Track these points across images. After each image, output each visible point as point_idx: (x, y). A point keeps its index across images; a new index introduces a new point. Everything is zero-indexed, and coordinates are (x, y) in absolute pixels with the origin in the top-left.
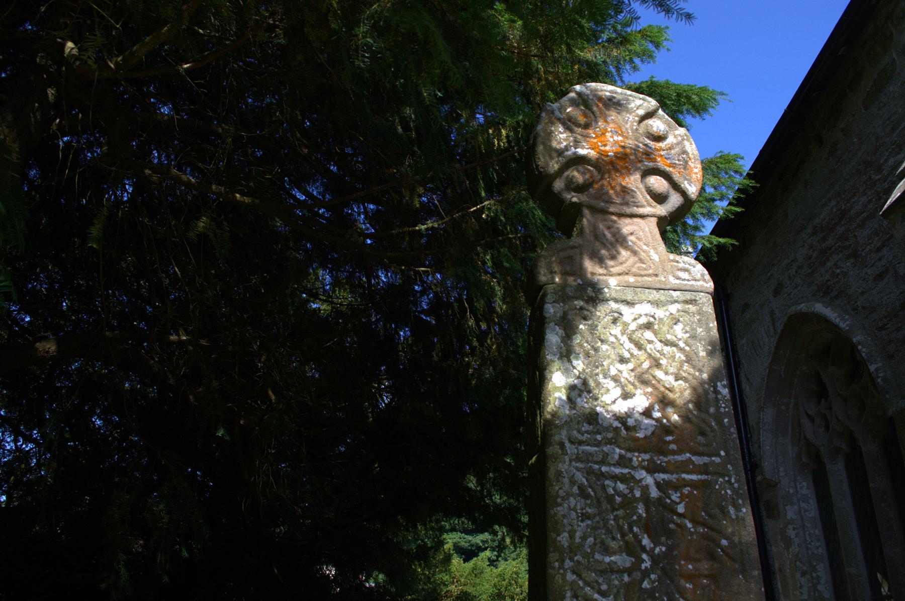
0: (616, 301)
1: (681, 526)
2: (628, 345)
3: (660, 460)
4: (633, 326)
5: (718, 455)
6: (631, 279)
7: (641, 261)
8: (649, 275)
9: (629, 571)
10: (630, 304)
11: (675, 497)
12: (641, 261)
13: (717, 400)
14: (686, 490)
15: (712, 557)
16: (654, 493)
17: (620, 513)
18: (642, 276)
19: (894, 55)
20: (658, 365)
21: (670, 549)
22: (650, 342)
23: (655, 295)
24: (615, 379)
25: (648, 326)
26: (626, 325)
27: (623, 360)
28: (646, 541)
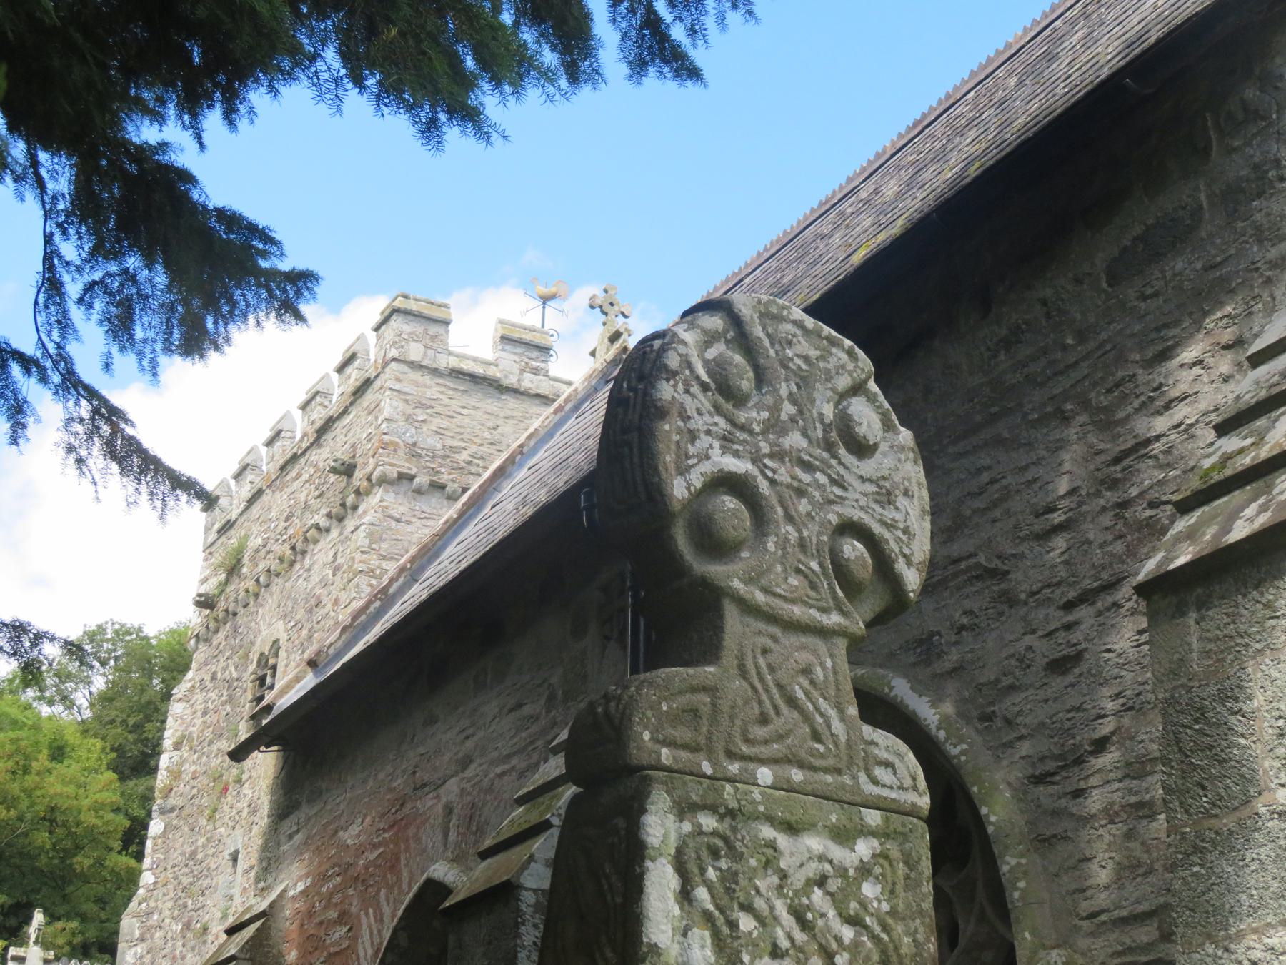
0: (770, 820)
2: (787, 919)
4: (798, 879)
6: (797, 775)
7: (816, 736)
8: (826, 770)
10: (792, 829)
12: (816, 736)
18: (815, 769)
19: (1203, 197)
25: (821, 881)
26: (784, 876)
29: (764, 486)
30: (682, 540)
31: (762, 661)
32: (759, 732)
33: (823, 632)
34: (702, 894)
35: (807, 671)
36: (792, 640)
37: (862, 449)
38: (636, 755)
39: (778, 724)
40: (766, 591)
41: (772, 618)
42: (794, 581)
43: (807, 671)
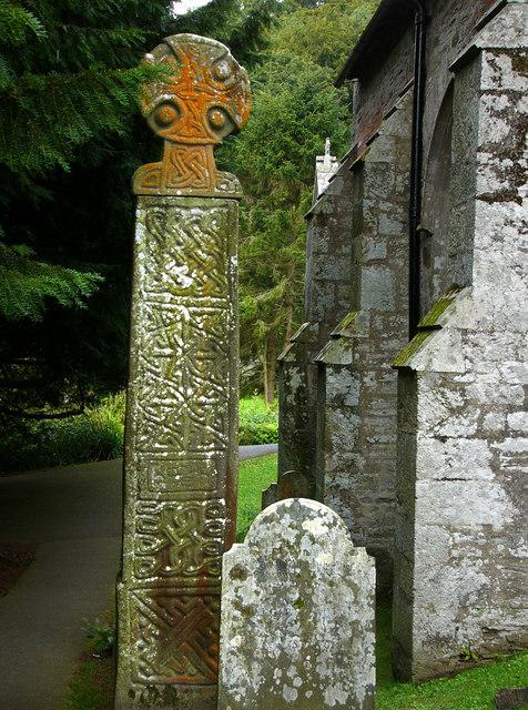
0: (179, 207)
1: (201, 335)
3: (192, 300)
4: (187, 222)
5: (226, 297)
7: (198, 178)
9: (170, 356)
10: (187, 208)
11: (198, 319)
12: (198, 178)
13: (229, 267)
14: (205, 317)
15: (214, 349)
16: (187, 318)
17: (169, 328)
20: (199, 246)
21: (193, 345)
22: (196, 232)
23: (200, 202)
24: (172, 255)
25: (197, 222)
27: (179, 244)
28: (181, 343)
29: (179, 100)
30: (152, 124)
31: (179, 158)
32: (178, 179)
33: (204, 145)
34: (154, 231)
35: (196, 158)
36: (192, 149)
37: (222, 79)
38: (136, 192)
39: (184, 177)
40: (180, 135)
41: (186, 144)
42: (192, 130)
43: (196, 158)
